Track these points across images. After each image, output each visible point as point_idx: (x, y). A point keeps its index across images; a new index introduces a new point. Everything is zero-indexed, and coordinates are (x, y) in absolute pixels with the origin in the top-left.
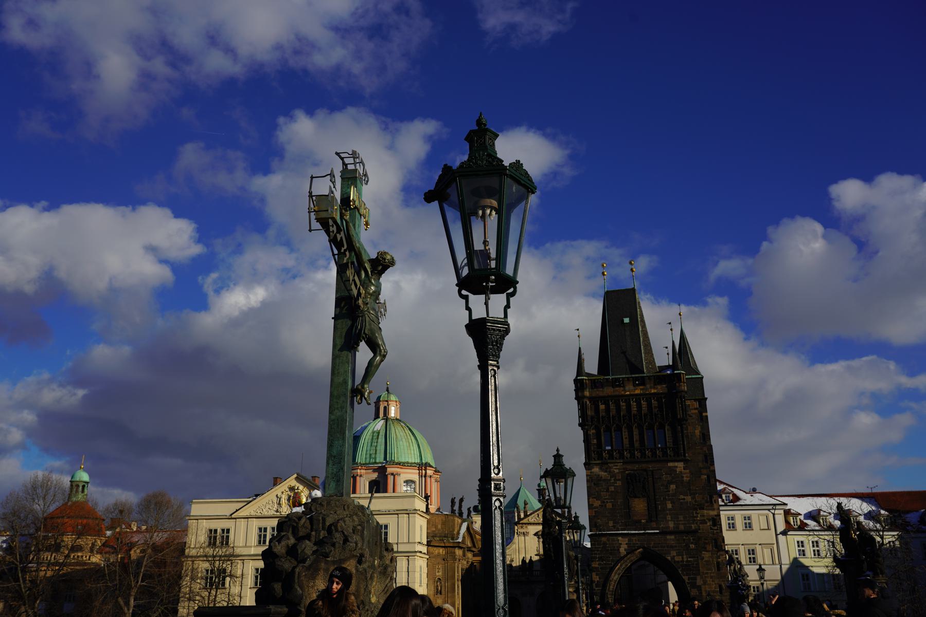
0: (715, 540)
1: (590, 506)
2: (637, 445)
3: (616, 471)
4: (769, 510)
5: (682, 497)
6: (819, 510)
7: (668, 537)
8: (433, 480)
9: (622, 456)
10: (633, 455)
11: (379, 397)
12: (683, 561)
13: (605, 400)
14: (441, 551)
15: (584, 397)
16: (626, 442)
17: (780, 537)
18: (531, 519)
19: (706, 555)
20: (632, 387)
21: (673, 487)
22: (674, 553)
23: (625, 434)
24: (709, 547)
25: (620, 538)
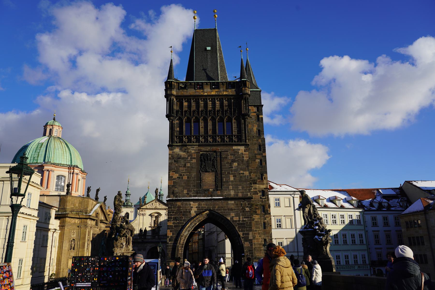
0: (264, 206)
1: (170, 178)
2: (210, 133)
3: (193, 151)
4: (291, 195)
5: (242, 172)
6: (319, 196)
7: (229, 202)
8: (80, 177)
9: (198, 140)
10: (206, 140)
11: (47, 123)
12: (239, 221)
13: (188, 98)
14: (77, 221)
15: (172, 95)
16: (202, 130)
17: (296, 211)
18: (148, 206)
19: (256, 217)
20: (209, 90)
21: (235, 164)
22: (233, 214)
23: (202, 124)
24: (259, 212)
25: (192, 203)
